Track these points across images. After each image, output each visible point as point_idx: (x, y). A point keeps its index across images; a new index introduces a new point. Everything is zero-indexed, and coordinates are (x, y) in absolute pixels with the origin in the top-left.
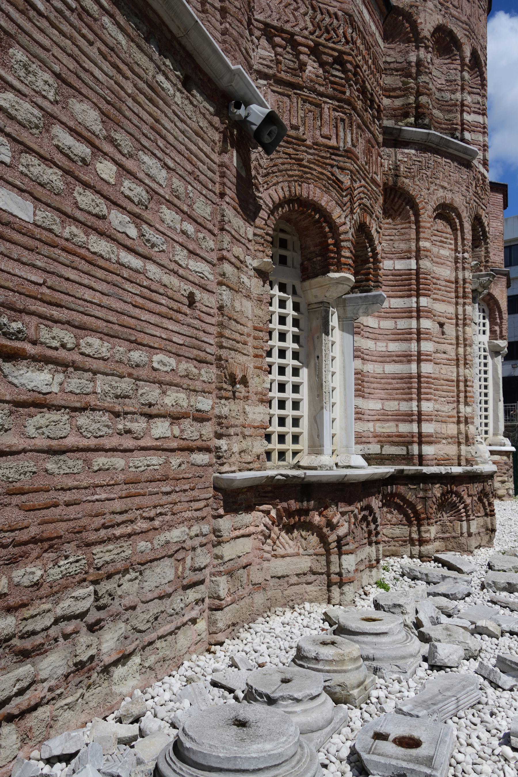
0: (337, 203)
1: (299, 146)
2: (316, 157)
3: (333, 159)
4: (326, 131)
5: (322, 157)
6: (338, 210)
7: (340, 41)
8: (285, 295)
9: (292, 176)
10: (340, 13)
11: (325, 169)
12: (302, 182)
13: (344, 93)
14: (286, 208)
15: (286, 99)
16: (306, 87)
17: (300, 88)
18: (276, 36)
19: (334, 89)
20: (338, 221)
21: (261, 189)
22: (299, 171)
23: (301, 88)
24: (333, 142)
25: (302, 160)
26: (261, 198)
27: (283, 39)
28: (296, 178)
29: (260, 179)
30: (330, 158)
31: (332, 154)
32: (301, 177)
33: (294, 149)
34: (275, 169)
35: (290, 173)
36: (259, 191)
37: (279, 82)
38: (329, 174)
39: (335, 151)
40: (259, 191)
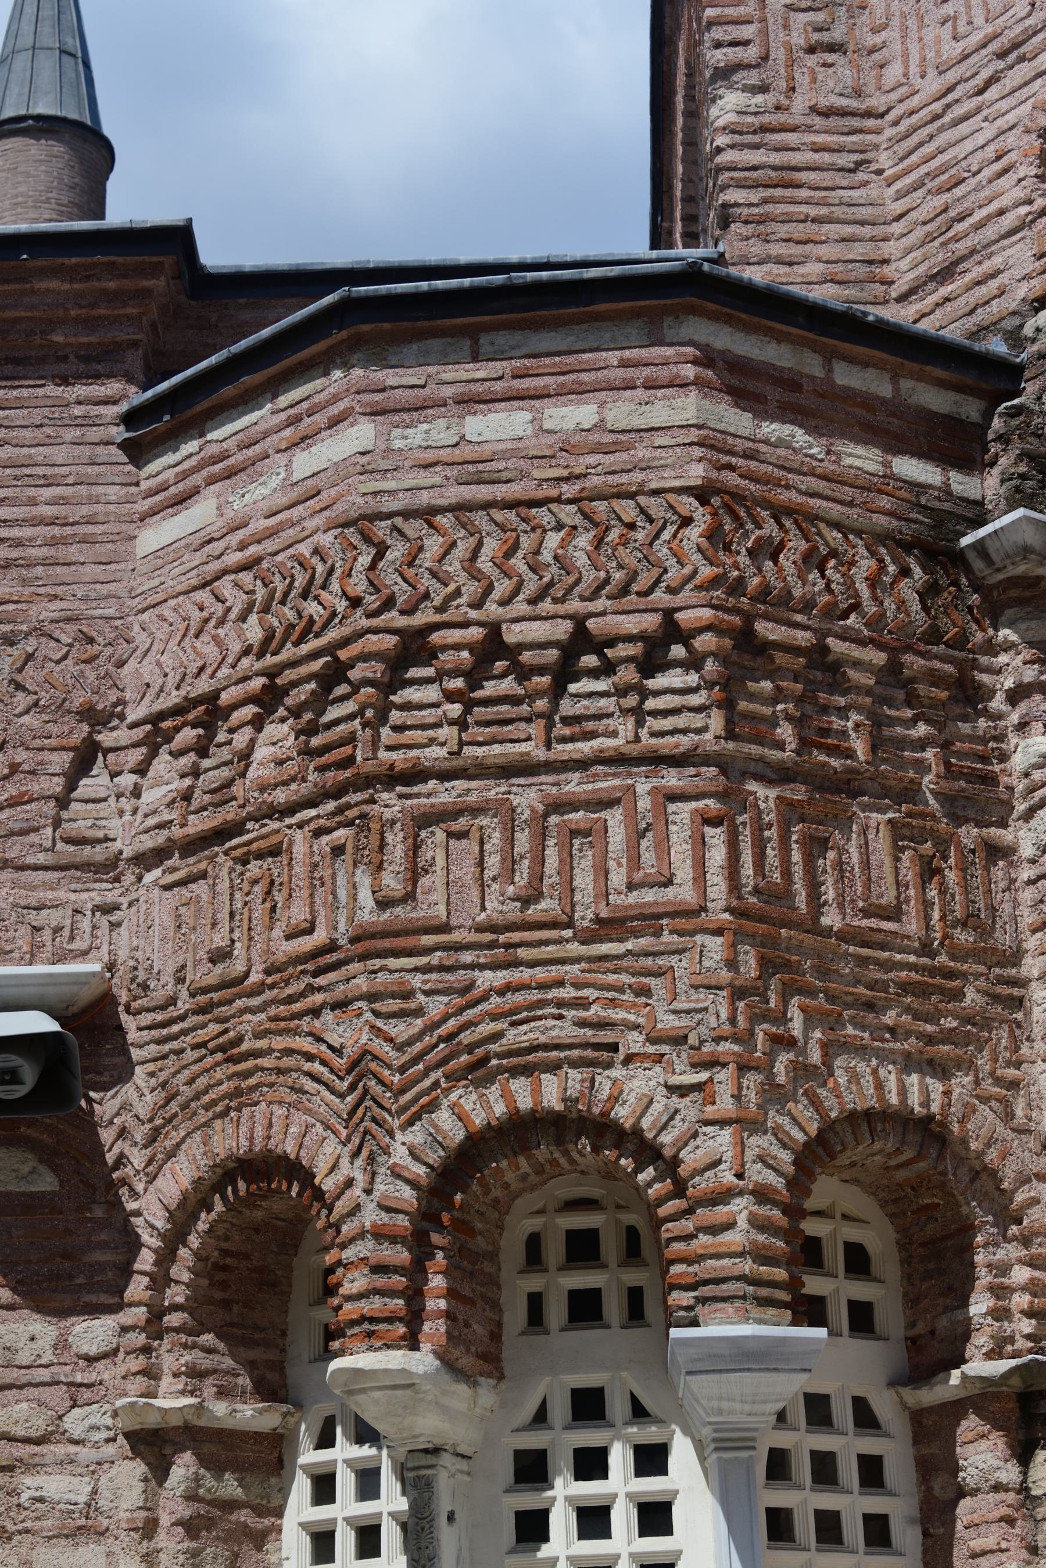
0: (327, 1127)
1: (230, 1002)
2: (272, 1011)
3: (320, 989)
4: (299, 913)
5: (290, 1000)
6: (331, 1147)
7: (334, 614)
8: (373, 1451)
9: (214, 1103)
10: (326, 539)
11: (296, 1032)
12: (239, 1109)
13: (350, 760)
14: (219, 1207)
15: (200, 888)
16: (251, 817)
17: (236, 828)
18: (177, 729)
19: (321, 769)
20: (328, 1185)
21: (140, 1187)
22: (229, 1078)
23: (236, 828)
24: (320, 936)
25: (239, 1040)
26: (138, 1213)
27: (194, 726)
28: (219, 1109)
29: (137, 1158)
30: (312, 989)
31: (316, 974)
32: (238, 1093)
33: (219, 1020)
34: (174, 1107)
35: (206, 1099)
36: (134, 1195)
37: (192, 846)
38: (306, 1044)
39: (333, 958)
40: (134, 1195)
